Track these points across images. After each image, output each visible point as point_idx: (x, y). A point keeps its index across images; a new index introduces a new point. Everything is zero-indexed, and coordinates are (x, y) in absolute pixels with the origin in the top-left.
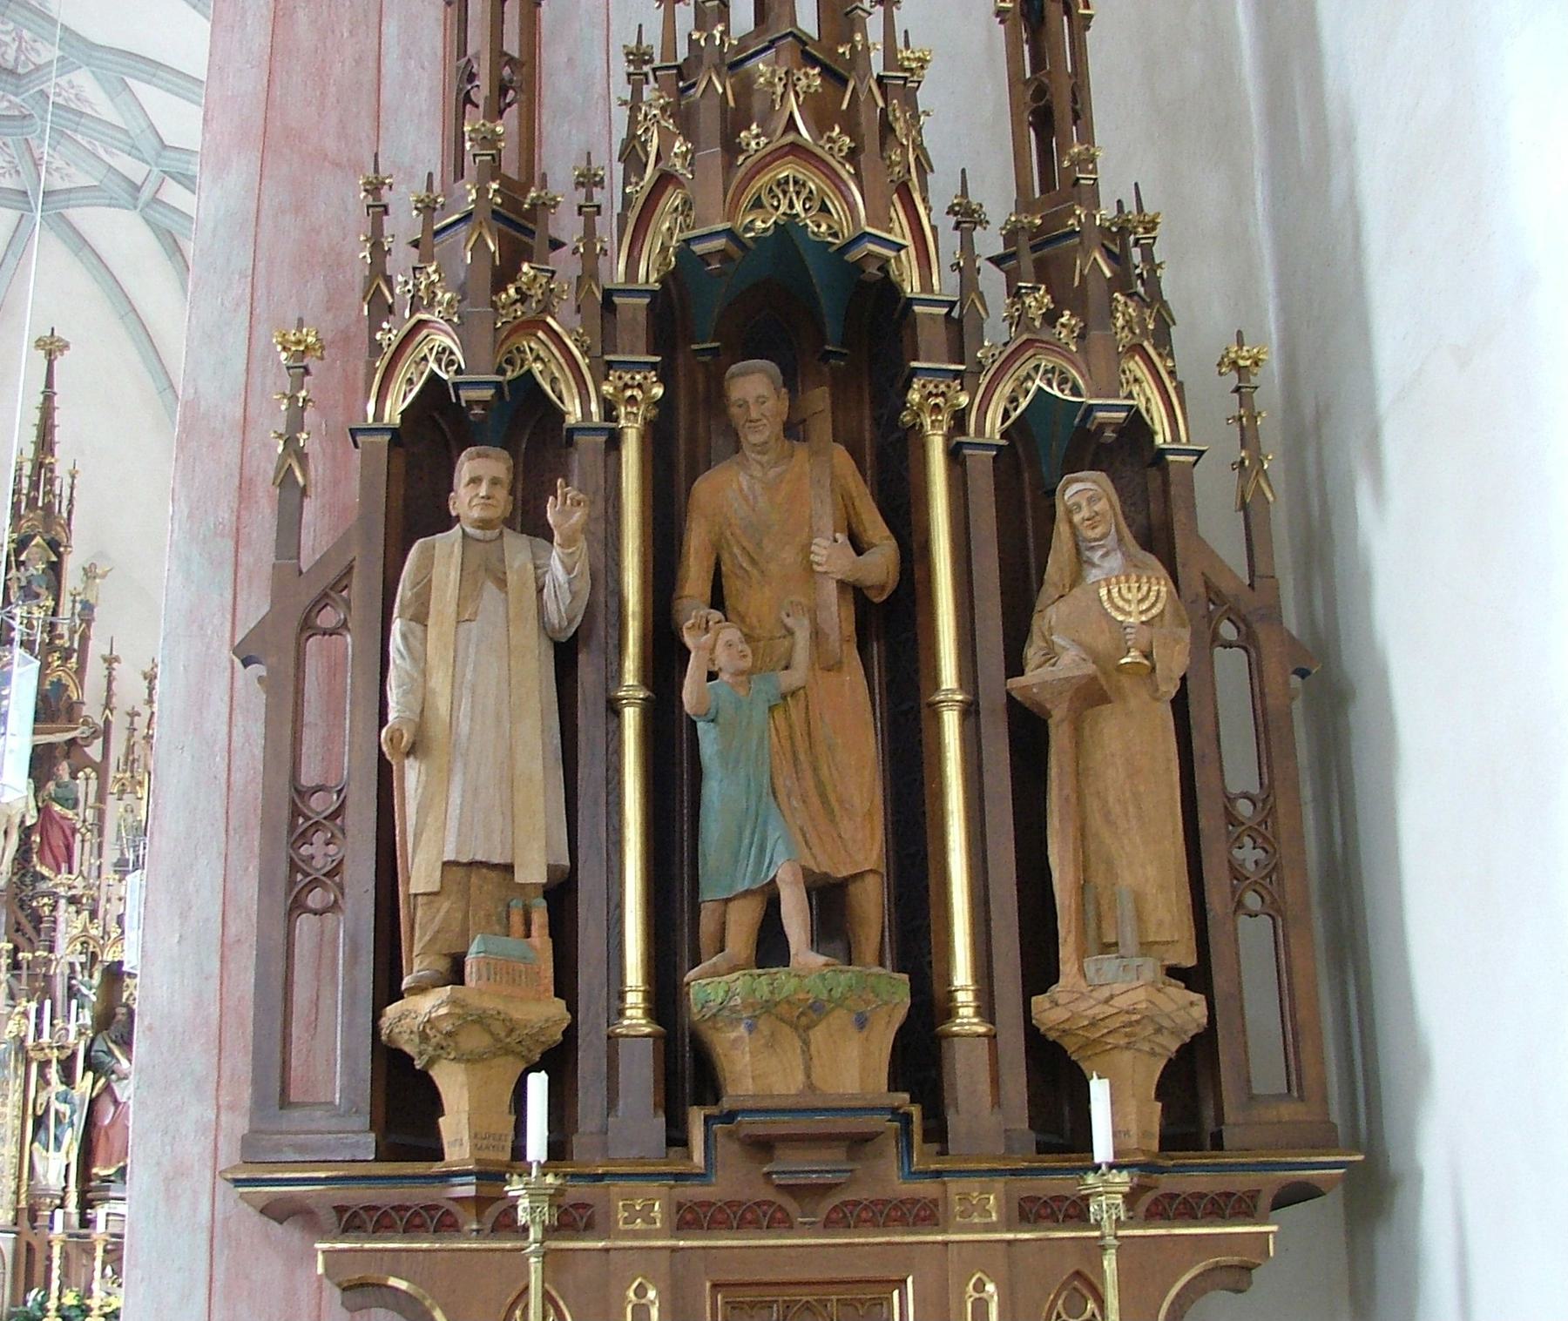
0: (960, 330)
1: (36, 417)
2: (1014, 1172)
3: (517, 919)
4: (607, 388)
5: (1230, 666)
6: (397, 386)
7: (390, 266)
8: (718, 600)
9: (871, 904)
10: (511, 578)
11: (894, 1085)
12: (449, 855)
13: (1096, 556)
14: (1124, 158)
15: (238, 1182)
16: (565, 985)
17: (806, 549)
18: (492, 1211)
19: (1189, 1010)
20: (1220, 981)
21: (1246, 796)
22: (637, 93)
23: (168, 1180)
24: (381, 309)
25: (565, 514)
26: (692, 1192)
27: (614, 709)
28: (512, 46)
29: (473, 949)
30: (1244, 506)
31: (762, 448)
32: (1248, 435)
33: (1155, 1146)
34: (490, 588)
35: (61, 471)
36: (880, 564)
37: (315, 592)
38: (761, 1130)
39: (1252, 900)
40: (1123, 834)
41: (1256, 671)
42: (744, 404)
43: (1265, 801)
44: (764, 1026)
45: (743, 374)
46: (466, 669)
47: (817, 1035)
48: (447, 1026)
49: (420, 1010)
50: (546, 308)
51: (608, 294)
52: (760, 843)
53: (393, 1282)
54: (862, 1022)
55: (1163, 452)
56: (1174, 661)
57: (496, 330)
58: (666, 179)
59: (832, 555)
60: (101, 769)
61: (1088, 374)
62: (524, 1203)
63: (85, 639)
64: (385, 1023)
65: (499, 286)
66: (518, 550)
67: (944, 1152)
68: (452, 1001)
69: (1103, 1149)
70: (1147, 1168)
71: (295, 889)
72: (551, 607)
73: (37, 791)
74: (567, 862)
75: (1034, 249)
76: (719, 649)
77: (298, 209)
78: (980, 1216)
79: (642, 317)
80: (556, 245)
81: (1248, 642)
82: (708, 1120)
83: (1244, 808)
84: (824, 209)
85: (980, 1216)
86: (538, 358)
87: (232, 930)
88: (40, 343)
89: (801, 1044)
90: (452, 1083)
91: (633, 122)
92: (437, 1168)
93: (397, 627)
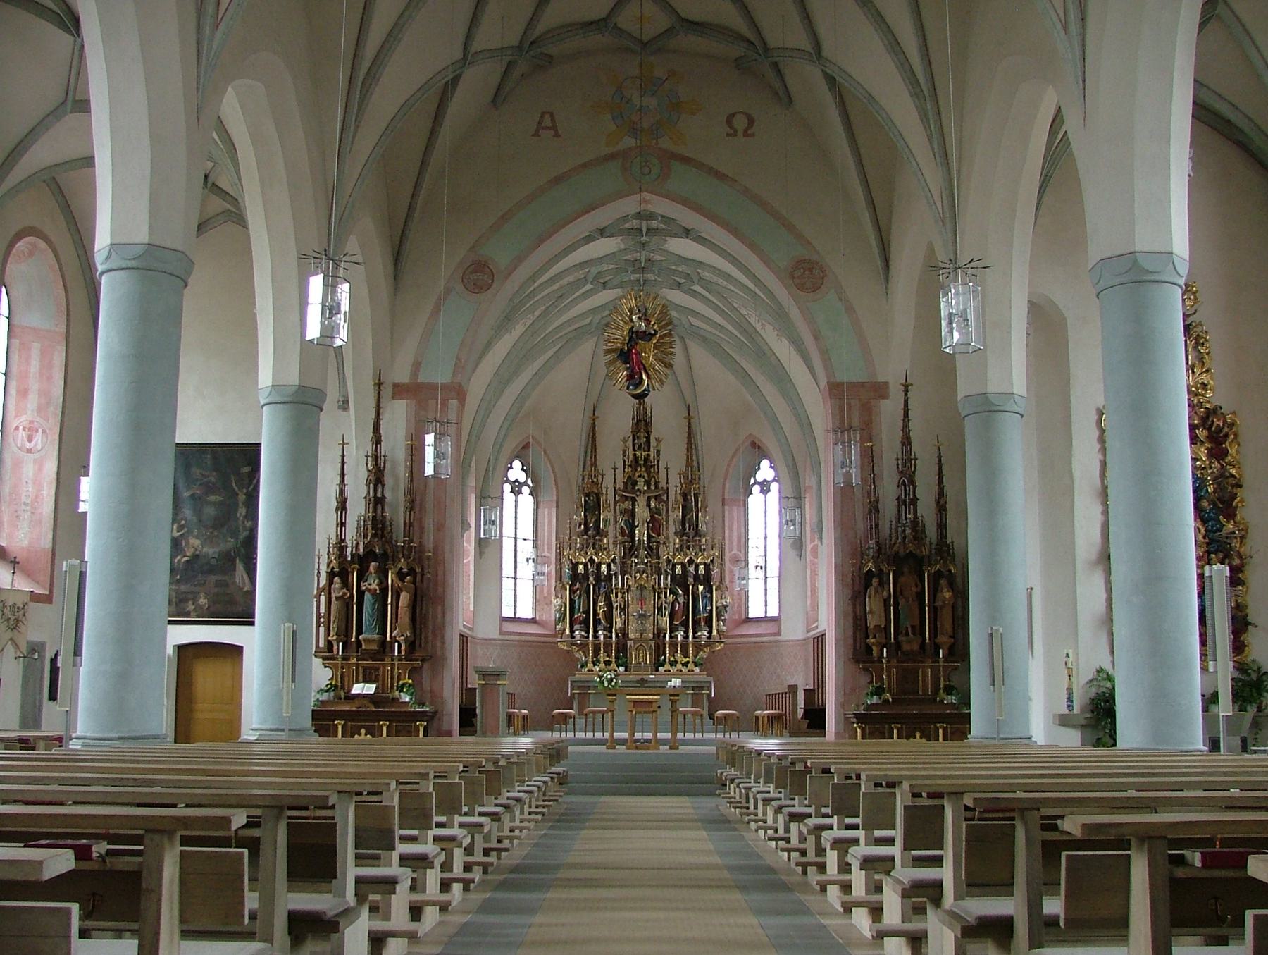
40: (946, 622)
46: (873, 604)
52: (906, 623)
60: (667, 502)
71: (856, 626)
78: (929, 663)
85: (929, 663)
89: (910, 645)
90: (874, 648)
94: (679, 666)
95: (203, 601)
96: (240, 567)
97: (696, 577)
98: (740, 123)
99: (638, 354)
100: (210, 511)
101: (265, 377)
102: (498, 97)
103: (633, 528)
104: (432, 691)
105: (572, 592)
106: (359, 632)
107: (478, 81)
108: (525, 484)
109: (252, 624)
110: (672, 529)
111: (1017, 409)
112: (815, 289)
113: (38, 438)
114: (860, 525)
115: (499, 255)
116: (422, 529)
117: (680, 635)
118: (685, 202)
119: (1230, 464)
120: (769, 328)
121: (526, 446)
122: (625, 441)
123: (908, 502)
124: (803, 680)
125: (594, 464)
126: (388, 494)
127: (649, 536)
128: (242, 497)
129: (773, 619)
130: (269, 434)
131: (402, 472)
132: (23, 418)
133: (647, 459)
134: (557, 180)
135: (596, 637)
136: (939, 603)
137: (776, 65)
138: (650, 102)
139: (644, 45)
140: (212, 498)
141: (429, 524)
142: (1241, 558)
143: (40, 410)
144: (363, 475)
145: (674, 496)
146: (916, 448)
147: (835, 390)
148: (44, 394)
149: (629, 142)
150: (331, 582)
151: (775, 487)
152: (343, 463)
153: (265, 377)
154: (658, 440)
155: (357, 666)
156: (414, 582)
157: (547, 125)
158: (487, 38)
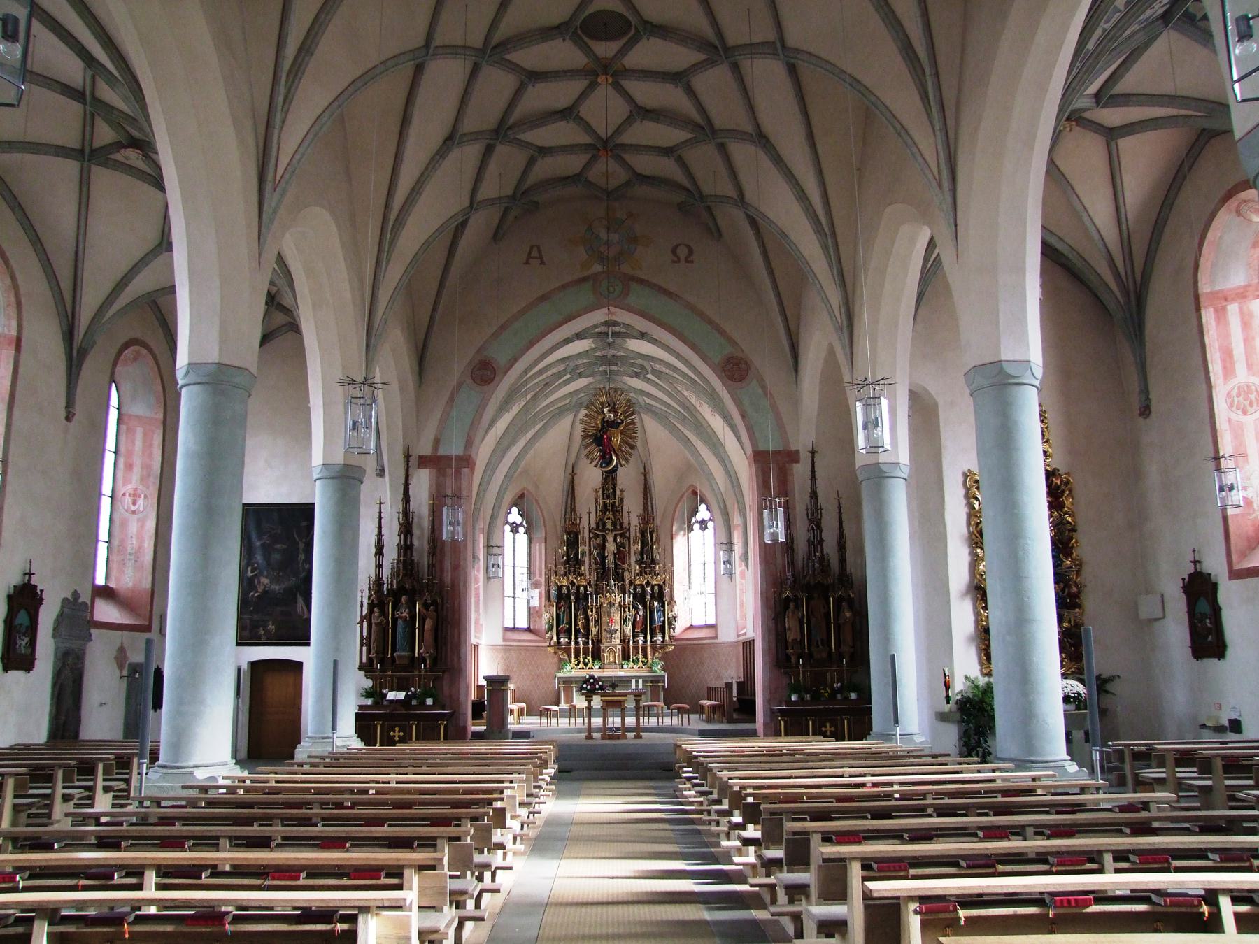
46: (791, 623)
71: (777, 640)
94: (640, 664)
95: (271, 627)
96: (300, 600)
97: (652, 596)
98: (682, 252)
99: (609, 439)
100: (276, 556)
101: (317, 458)
102: (497, 235)
103: (603, 558)
104: (451, 696)
105: (558, 608)
106: (394, 650)
107: (480, 224)
108: (521, 525)
109: (308, 644)
110: (633, 559)
111: (901, 475)
112: (742, 379)
113: (141, 501)
114: (780, 561)
115: (499, 355)
116: (442, 570)
117: (641, 640)
118: (644, 315)
119: (1066, 513)
120: (705, 406)
121: (522, 496)
122: (596, 491)
123: (816, 542)
124: (733, 674)
125: (573, 510)
126: (416, 542)
127: (616, 565)
128: (302, 546)
129: (712, 626)
130: (320, 497)
131: (426, 523)
132: (130, 486)
133: (613, 505)
134: (544, 298)
135: (577, 643)
136: (841, 621)
137: (709, 209)
138: (615, 237)
139: (609, 193)
140: (278, 546)
141: (448, 564)
142: (1077, 586)
143: (143, 480)
144: (396, 527)
145: (634, 533)
146: (821, 500)
147: (759, 457)
148: (147, 467)
149: (597, 268)
150: (371, 611)
151: (710, 525)
152: (380, 518)
153: (317, 458)
154: (622, 491)
155: (392, 676)
156: (436, 611)
157: (535, 256)
158: (488, 190)
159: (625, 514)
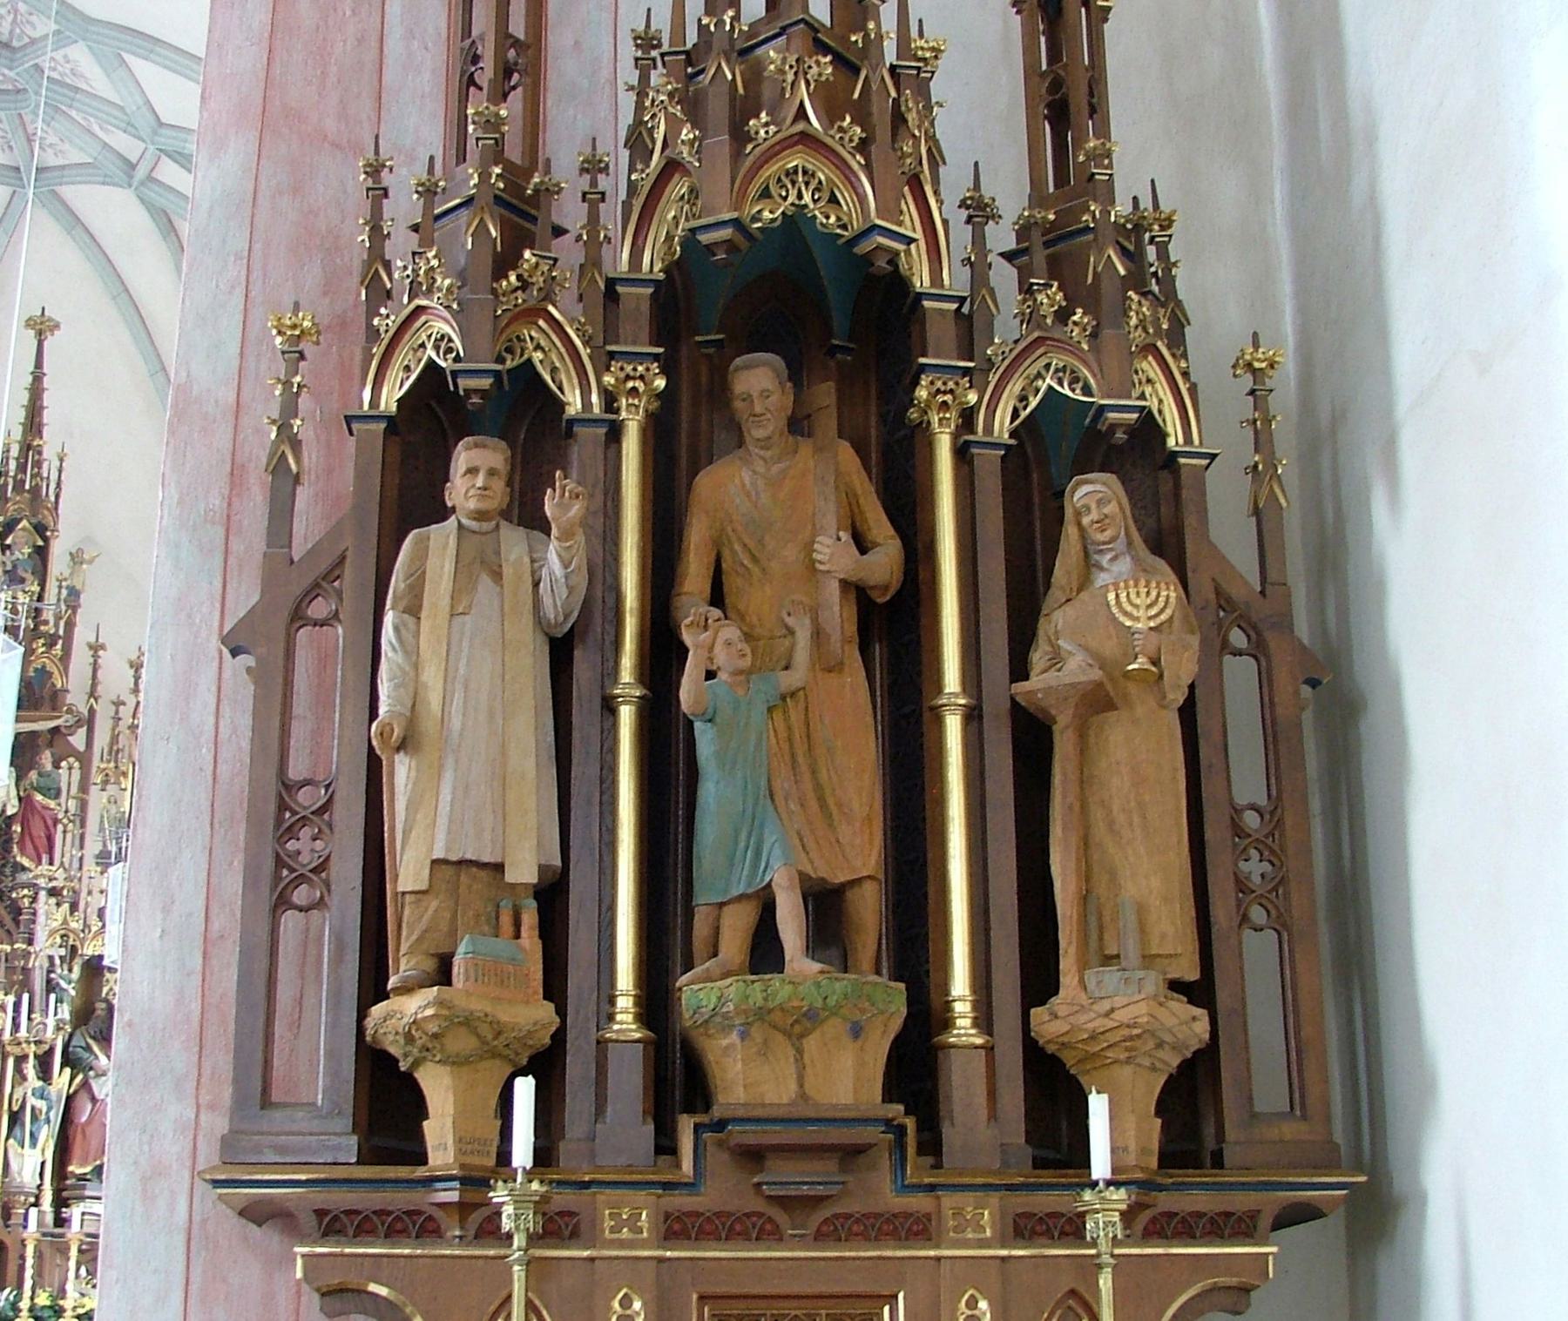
0: (970, 327)
1: (24, 398)
2: (1010, 1188)
3: (506, 920)
4: (608, 379)
5: (1240, 674)
6: (394, 373)
7: (389, 250)
8: (717, 598)
9: (868, 910)
10: (507, 571)
11: (888, 1097)
12: (439, 853)
13: (1105, 560)
14: (1141, 153)
15: (217, 1183)
16: (555, 987)
17: (809, 548)
18: (476, 1218)
19: (1190, 1025)
20: (1223, 997)
21: (1253, 807)
22: (644, 78)
23: (145, 1180)
24: (379, 294)
25: (563, 507)
26: (680, 1201)
27: (609, 708)
28: (518, 28)
29: (461, 949)
30: (1257, 512)
31: (765, 443)
32: (1262, 439)
33: (1154, 1162)
34: (485, 581)
35: (50, 453)
36: (884, 563)
37: (307, 582)
38: (751, 1140)
39: (1257, 914)
40: (1127, 844)
41: (1266, 680)
42: (748, 398)
43: (1273, 813)
44: (757, 1033)
45: (748, 367)
46: (459, 665)
47: (811, 1044)
48: (433, 1028)
49: (406, 1011)
50: (548, 296)
51: (611, 283)
53: (373, 1288)
54: (857, 1031)
55: (1175, 454)
56: (1182, 668)
57: (496, 317)
58: (672, 167)
59: (834, 554)
60: (84, 759)
61: (1100, 373)
62: (508, 1210)
63: (70, 625)
64: (370, 1023)
65: (499, 273)
66: (514, 543)
67: (938, 1165)
68: (439, 1003)
69: (1100, 1166)
70: (1145, 1185)
71: (280, 885)
72: (547, 601)
73: (18, 780)
74: (558, 862)
75: (1047, 245)
76: (718, 648)
77: (296, 190)
78: (974, 1231)
79: (645, 307)
80: (559, 232)
81: (1258, 650)
82: (697, 1128)
83: (1251, 820)
84: (833, 200)
85: (974, 1231)
86: (538, 347)
87: (216, 926)
88: (30, 323)
90: (437, 1086)
91: (639, 108)
92: (421, 1172)
93: (389, 619)
159: (80, 658)
